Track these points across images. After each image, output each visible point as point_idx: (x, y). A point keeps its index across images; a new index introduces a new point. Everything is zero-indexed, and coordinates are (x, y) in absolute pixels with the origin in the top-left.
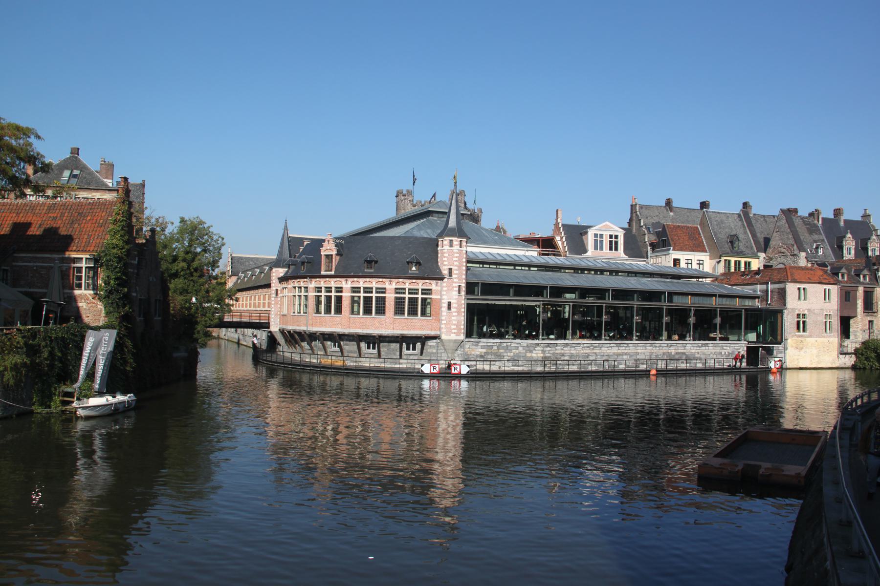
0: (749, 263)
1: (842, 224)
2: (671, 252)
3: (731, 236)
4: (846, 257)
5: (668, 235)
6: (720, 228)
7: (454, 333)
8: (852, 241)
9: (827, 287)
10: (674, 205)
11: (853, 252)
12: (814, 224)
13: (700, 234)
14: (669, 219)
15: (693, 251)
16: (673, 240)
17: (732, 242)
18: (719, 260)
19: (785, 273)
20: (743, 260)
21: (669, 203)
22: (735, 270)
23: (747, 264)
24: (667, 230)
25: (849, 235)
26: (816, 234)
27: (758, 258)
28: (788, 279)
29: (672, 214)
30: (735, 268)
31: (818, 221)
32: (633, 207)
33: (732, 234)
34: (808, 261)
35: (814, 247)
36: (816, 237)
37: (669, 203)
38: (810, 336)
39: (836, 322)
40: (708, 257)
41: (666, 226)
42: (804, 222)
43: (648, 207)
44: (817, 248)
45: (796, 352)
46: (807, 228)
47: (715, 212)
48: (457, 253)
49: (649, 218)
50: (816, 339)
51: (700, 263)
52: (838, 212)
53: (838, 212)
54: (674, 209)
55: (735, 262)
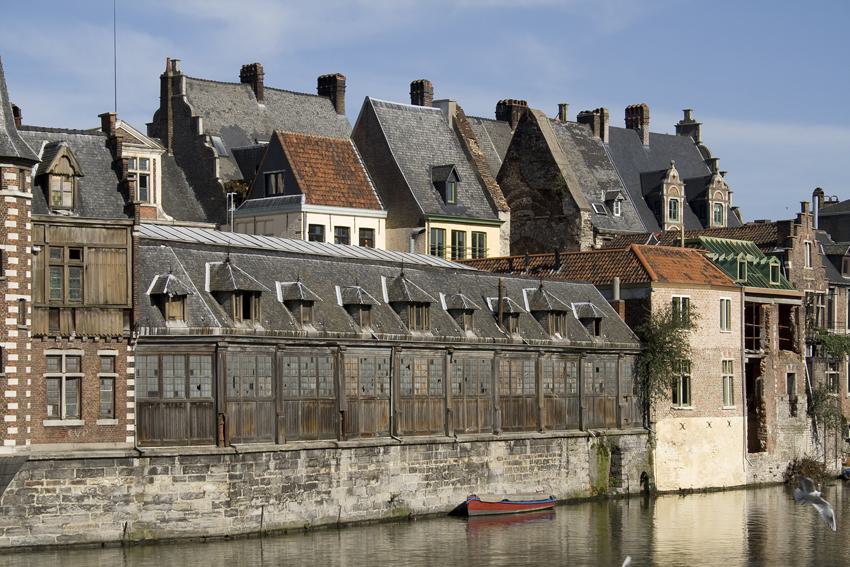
0: (482, 235)
1: (646, 142)
2: (305, 207)
3: (434, 168)
4: (669, 225)
5: (291, 162)
6: (409, 148)
7: (14, 437)
8: (680, 185)
9: (727, 295)
10: (267, 81)
11: (681, 211)
12: (595, 143)
13: (356, 161)
14: (255, 120)
15: (351, 205)
16: (302, 177)
17: (440, 186)
18: (420, 229)
19: (635, 264)
20: (469, 229)
21: (251, 76)
22: (474, 256)
23: (479, 240)
24: (284, 147)
25: (674, 172)
26: (602, 166)
27: (498, 224)
28: (650, 278)
29: (261, 106)
30: (474, 250)
31: (602, 136)
32: (171, 82)
33: (436, 163)
34: (596, 232)
35: (603, 199)
36: (602, 174)
37: (251, 76)
38: (697, 414)
39: (738, 375)
40: (383, 222)
41: (281, 138)
42: (574, 136)
43: (205, 84)
44: (609, 203)
45: (673, 452)
46: (582, 152)
47: (392, 106)
48: (15, 206)
49: (213, 114)
50: (708, 419)
51: (367, 237)
52: (636, 116)
53: (636, 116)
54: (265, 93)
55: (474, 234)
